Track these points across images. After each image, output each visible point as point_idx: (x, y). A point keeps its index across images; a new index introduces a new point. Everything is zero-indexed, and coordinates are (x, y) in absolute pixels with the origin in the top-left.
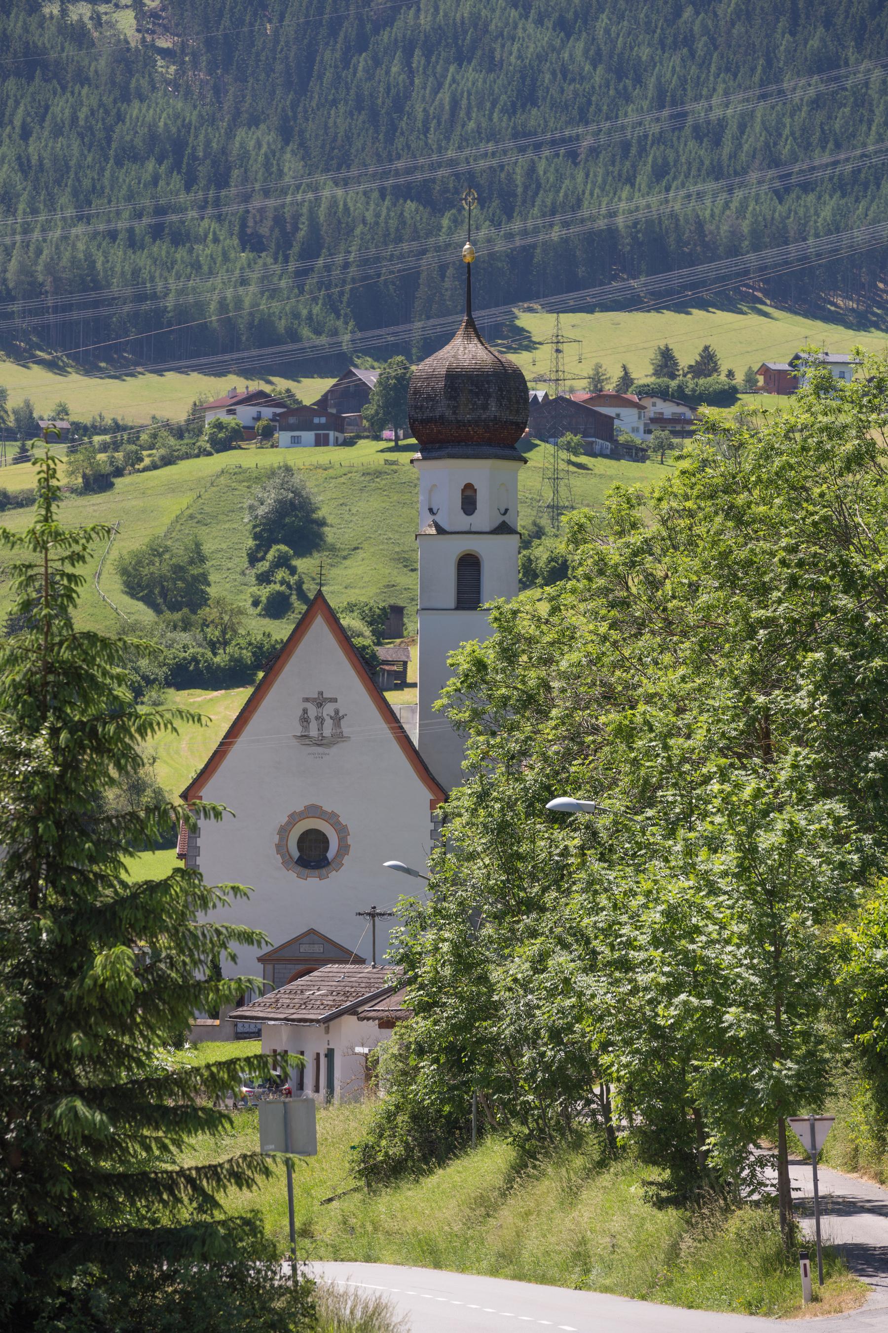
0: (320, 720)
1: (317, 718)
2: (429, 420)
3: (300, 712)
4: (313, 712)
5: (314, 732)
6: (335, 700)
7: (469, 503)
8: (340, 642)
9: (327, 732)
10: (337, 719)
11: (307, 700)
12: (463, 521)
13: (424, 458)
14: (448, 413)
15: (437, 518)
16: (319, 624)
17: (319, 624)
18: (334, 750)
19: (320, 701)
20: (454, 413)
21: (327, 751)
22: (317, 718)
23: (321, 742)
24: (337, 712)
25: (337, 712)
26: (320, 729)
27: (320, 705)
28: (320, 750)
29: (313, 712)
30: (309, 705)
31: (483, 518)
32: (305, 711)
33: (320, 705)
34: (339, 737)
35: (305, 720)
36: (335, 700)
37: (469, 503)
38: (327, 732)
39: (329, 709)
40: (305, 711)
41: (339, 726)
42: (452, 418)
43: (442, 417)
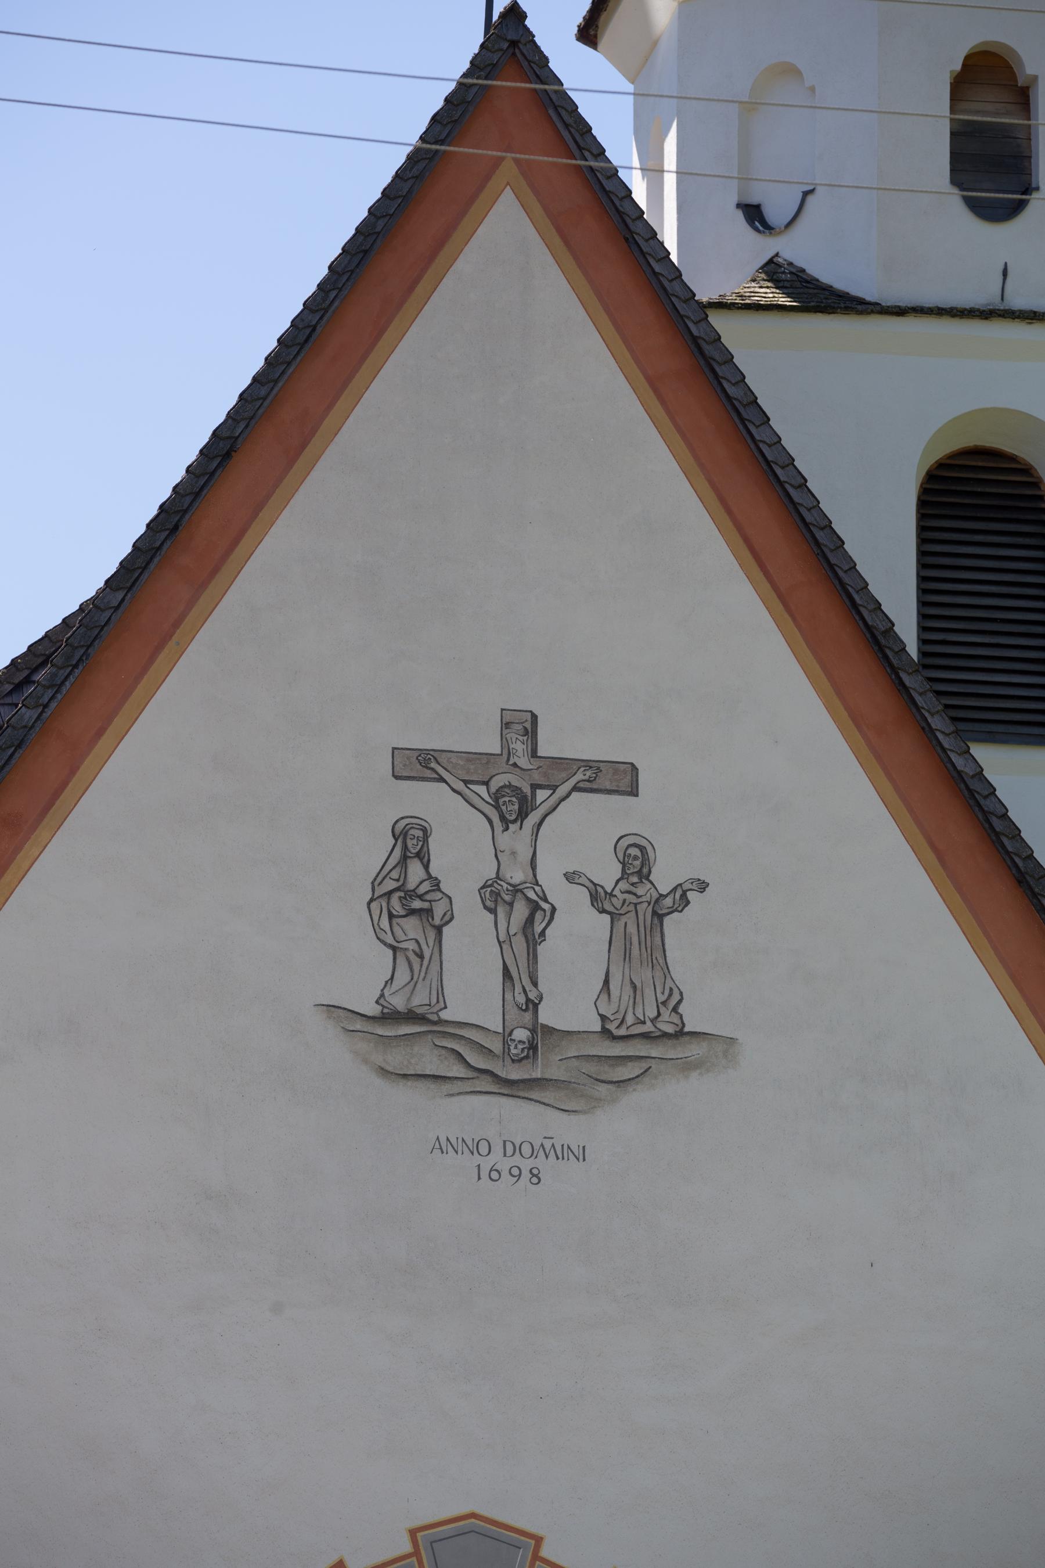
0: (522, 910)
1: (495, 896)
3: (376, 850)
4: (464, 848)
5: (471, 985)
6: (625, 780)
8: (654, 387)
9: (571, 1002)
10: (641, 904)
11: (421, 765)
16: (505, 248)
18: (616, 1127)
19: (520, 782)
21: (566, 1129)
22: (495, 896)
23: (522, 1061)
24: (636, 861)
25: (636, 861)
26: (521, 980)
28: (522, 1119)
29: (464, 848)
30: (434, 803)
32: (411, 842)
34: (650, 1038)
35: (407, 899)
36: (625, 780)
38: (571, 1002)
39: (578, 839)
40: (411, 842)
41: (656, 955)
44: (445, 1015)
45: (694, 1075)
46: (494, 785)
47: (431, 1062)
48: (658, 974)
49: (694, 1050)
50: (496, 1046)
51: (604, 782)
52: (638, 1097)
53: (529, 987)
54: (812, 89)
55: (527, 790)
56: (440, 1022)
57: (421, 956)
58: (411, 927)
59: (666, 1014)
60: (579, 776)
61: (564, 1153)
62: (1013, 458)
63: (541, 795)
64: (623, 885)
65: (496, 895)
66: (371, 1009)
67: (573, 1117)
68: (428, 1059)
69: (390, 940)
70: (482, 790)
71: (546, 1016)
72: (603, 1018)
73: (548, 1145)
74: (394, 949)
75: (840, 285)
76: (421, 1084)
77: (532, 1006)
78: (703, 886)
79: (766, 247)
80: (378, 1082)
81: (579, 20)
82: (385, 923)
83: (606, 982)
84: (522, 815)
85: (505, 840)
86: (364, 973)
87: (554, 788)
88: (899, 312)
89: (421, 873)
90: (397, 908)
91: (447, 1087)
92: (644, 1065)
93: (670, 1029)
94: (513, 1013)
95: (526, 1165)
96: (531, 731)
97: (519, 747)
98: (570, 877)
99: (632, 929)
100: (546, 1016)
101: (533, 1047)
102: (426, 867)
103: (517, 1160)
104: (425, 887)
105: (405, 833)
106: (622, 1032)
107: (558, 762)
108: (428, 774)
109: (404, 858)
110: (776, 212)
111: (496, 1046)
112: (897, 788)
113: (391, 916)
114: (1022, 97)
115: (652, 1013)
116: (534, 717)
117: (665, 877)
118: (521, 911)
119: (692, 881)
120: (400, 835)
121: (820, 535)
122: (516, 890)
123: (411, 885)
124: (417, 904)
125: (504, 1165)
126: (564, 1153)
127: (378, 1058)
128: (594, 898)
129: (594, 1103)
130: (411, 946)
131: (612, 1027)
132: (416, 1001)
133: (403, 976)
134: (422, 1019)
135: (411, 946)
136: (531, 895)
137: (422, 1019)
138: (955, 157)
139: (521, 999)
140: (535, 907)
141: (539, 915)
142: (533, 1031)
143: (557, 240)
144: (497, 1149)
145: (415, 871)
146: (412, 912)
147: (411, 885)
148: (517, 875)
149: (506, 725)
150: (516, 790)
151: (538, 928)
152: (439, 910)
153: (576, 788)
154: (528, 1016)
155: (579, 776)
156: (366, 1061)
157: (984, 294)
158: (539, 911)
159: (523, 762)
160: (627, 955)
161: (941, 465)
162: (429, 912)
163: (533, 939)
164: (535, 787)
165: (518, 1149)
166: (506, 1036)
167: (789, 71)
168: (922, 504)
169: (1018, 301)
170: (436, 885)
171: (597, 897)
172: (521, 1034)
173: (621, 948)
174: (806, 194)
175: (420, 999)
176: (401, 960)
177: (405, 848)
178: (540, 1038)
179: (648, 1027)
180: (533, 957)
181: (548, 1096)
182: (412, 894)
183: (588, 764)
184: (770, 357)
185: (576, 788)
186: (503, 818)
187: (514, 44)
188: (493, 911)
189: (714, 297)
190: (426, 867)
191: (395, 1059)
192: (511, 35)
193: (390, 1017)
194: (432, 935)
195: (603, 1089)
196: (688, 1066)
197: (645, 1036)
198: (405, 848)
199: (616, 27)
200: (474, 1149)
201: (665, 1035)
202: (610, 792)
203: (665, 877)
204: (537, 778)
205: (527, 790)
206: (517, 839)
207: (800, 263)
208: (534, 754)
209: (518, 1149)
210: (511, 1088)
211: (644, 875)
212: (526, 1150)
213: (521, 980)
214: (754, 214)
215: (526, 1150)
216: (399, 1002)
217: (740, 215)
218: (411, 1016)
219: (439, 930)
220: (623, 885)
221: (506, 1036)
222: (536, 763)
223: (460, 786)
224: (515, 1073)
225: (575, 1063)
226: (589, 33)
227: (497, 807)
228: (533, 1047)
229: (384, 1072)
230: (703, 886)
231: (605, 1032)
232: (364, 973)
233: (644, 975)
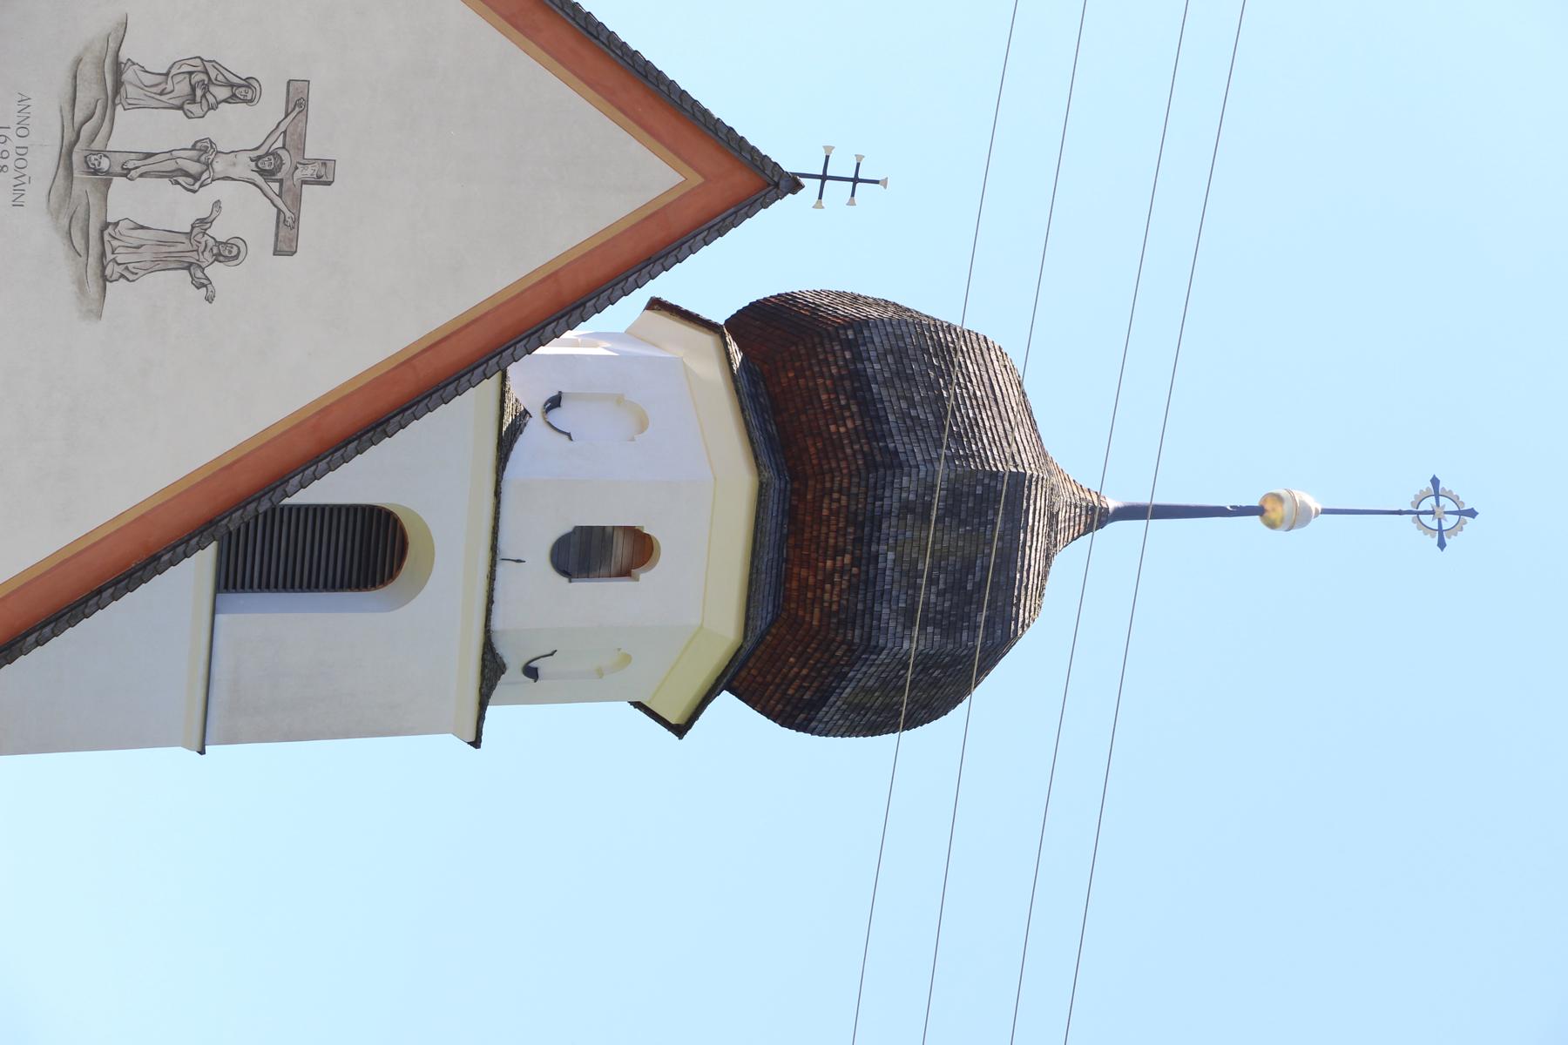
0: (194, 169)
1: (204, 150)
2: (869, 407)
4: (239, 129)
5: (141, 129)
6: (285, 246)
7: (588, 553)
8: (551, 277)
9: (128, 201)
10: (197, 254)
11: (297, 101)
12: (533, 535)
13: (734, 378)
14: (907, 486)
15: (535, 429)
16: (645, 176)
17: (645, 176)
18: (35, 232)
19: (282, 170)
20: (907, 508)
21: (36, 192)
22: (204, 150)
23: (85, 164)
24: (228, 252)
25: (228, 252)
26: (143, 165)
27: (267, 167)
28: (44, 160)
29: (239, 129)
30: (270, 109)
31: (540, 602)
32: (243, 91)
33: (267, 167)
34: (102, 258)
35: (203, 86)
36: (285, 246)
37: (588, 553)
38: (128, 201)
39: (243, 211)
40: (243, 91)
42: (891, 501)
43: (894, 462)
44: (119, 109)
45: (74, 288)
46: (283, 153)
47: (87, 95)
48: (148, 265)
49: (93, 288)
50: (97, 145)
51: (283, 232)
52: (59, 247)
53: (139, 171)
54: (633, 440)
55: (279, 176)
56: (114, 105)
57: (161, 94)
58: (183, 88)
59: (119, 269)
60: (288, 214)
61: (19, 191)
62: (400, 566)
63: (275, 186)
64: (211, 242)
65: (205, 151)
66: (123, 57)
67: (45, 199)
68: (88, 94)
69: (173, 72)
70: (279, 144)
71: (118, 182)
72: (117, 224)
73: (25, 179)
74: (167, 74)
75: (513, 455)
76: (69, 89)
77: (126, 173)
78: (209, 299)
79: (536, 410)
80: (70, 59)
81: (664, 298)
82: (186, 68)
83: (142, 227)
84: (261, 172)
85: (244, 158)
86: (151, 51)
87: (280, 196)
88: (497, 494)
89: (220, 98)
90: (197, 78)
91: (67, 108)
92: (82, 252)
93: (108, 272)
94: (120, 158)
95: (10, 162)
96: (319, 181)
97: (309, 172)
98: (217, 204)
99: (180, 247)
100: (118, 182)
101: (96, 172)
102: (225, 101)
103: (14, 156)
104: (211, 100)
105: (249, 86)
106: (106, 237)
107: (298, 199)
108: (291, 106)
109: (232, 85)
110: (556, 416)
111: (97, 145)
112: (275, 439)
113: (191, 73)
114: (625, 573)
115: (120, 259)
116: (329, 183)
117: (216, 271)
118: (194, 168)
119: (214, 292)
120: (248, 83)
121: (451, 388)
122: (208, 165)
123: (212, 89)
124: (199, 93)
125: (9, 146)
126: (19, 191)
127: (88, 58)
128: (202, 221)
129: (55, 214)
130: (169, 88)
131: (110, 230)
132: (130, 88)
133: (148, 80)
134: (116, 92)
135: (169, 88)
136: (205, 176)
137: (116, 92)
138: (591, 528)
139: (130, 165)
140: (196, 178)
141: (190, 180)
142: (107, 173)
143: (649, 212)
144: (22, 142)
145: (222, 93)
146: (193, 89)
147: (212, 89)
148: (219, 166)
149: (324, 163)
150: (279, 168)
151: (181, 179)
152: (195, 108)
153: (279, 211)
154: (118, 169)
155: (288, 214)
156: (86, 49)
157: (507, 547)
158: (195, 181)
159: (299, 174)
160: (162, 243)
161: (396, 520)
162: (193, 101)
163: (174, 175)
164: (281, 181)
165: (21, 157)
166: (103, 153)
167: (643, 425)
168: (372, 508)
169: (501, 569)
170: (211, 108)
171: (203, 223)
172: (105, 164)
173: (167, 239)
174: (569, 435)
175: (130, 91)
176: (159, 79)
177: (240, 86)
178: (103, 179)
179: (110, 256)
180: (161, 175)
181: (60, 181)
182: (206, 89)
183: (296, 220)
184: (472, 409)
185: (279, 211)
186: (259, 158)
187: (777, 185)
188: (193, 148)
189: (509, 374)
190: (225, 101)
191: (88, 71)
192: (782, 183)
193: (118, 68)
194: (177, 102)
195: (65, 222)
196: (81, 284)
197: (103, 254)
198: (240, 86)
199: (659, 318)
200: (21, 126)
201: (104, 268)
202: (277, 235)
203: (216, 271)
204: (287, 184)
205: (279, 176)
206: (244, 168)
207: (526, 430)
208: (304, 182)
209: (21, 157)
210: (67, 154)
211: (218, 257)
212: (21, 163)
213: (143, 165)
214: (555, 402)
215: (21, 163)
216: (128, 75)
217: (555, 393)
218: (118, 84)
219: (180, 108)
220: (211, 242)
221: (103, 153)
222: (298, 183)
223: (282, 128)
224: (77, 158)
225: (84, 202)
226: (656, 304)
227: (267, 154)
228: (96, 172)
229: (78, 61)
230: (209, 299)
231: (106, 225)
232: (151, 51)
233: (147, 255)
